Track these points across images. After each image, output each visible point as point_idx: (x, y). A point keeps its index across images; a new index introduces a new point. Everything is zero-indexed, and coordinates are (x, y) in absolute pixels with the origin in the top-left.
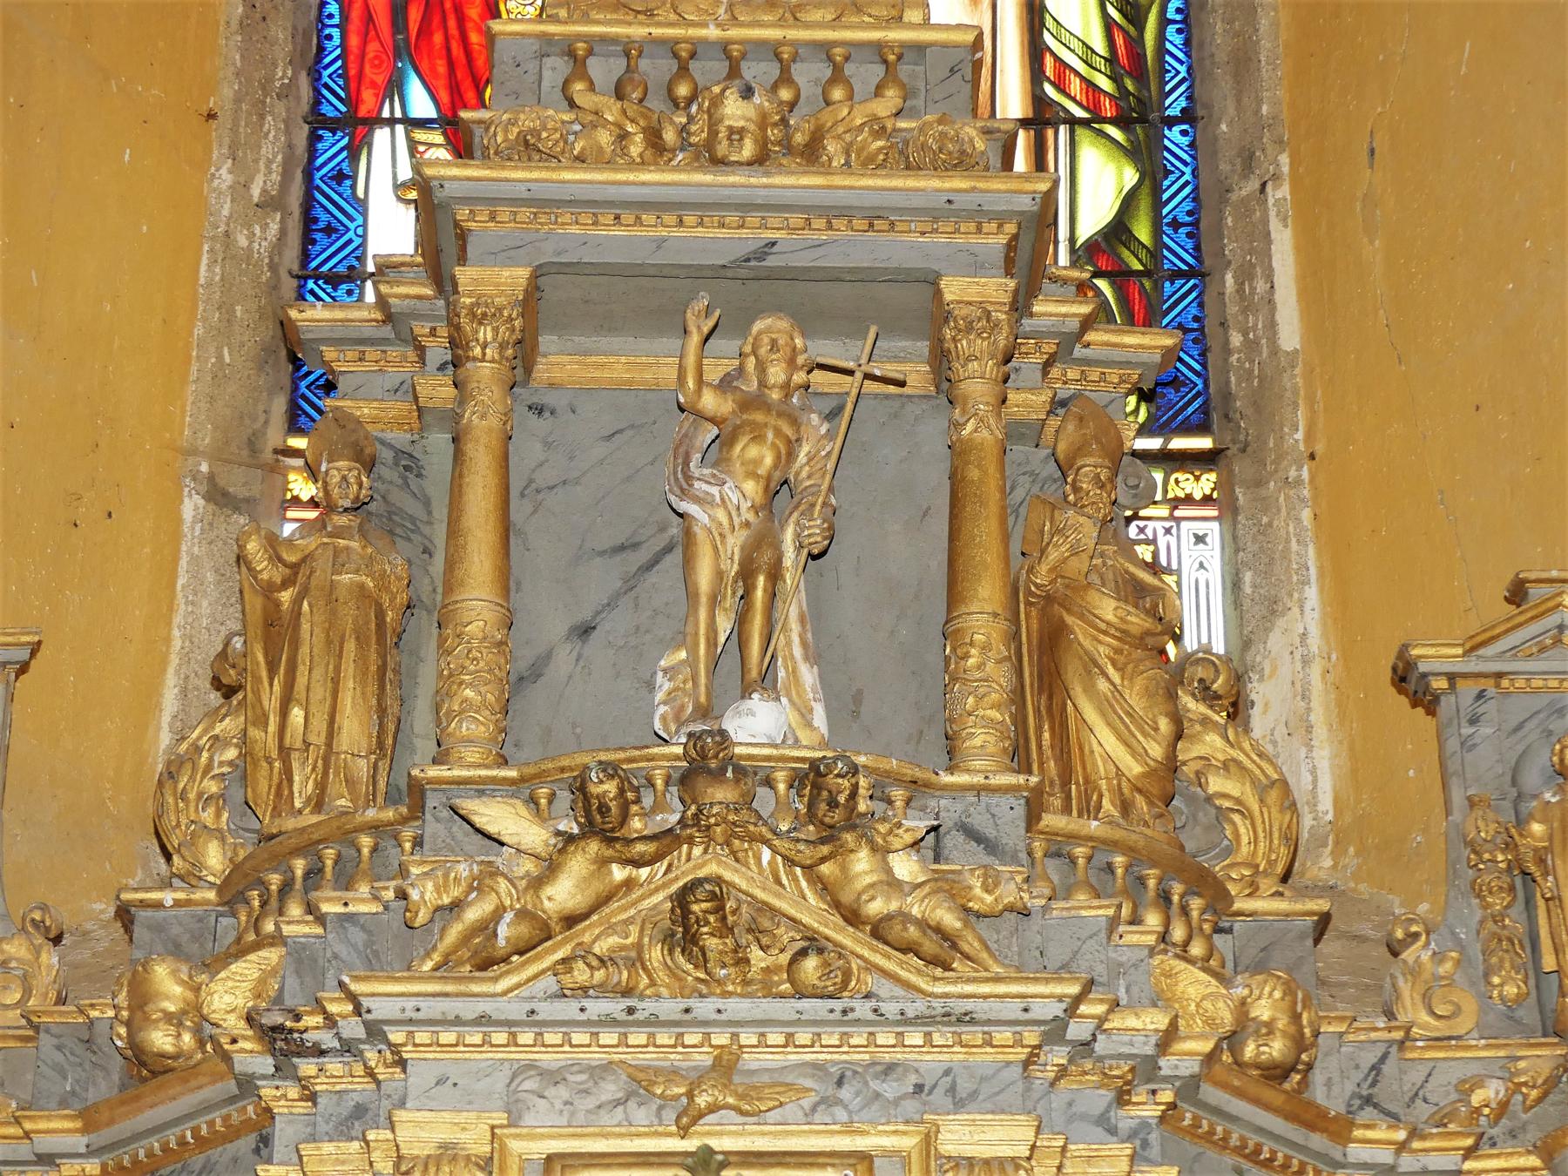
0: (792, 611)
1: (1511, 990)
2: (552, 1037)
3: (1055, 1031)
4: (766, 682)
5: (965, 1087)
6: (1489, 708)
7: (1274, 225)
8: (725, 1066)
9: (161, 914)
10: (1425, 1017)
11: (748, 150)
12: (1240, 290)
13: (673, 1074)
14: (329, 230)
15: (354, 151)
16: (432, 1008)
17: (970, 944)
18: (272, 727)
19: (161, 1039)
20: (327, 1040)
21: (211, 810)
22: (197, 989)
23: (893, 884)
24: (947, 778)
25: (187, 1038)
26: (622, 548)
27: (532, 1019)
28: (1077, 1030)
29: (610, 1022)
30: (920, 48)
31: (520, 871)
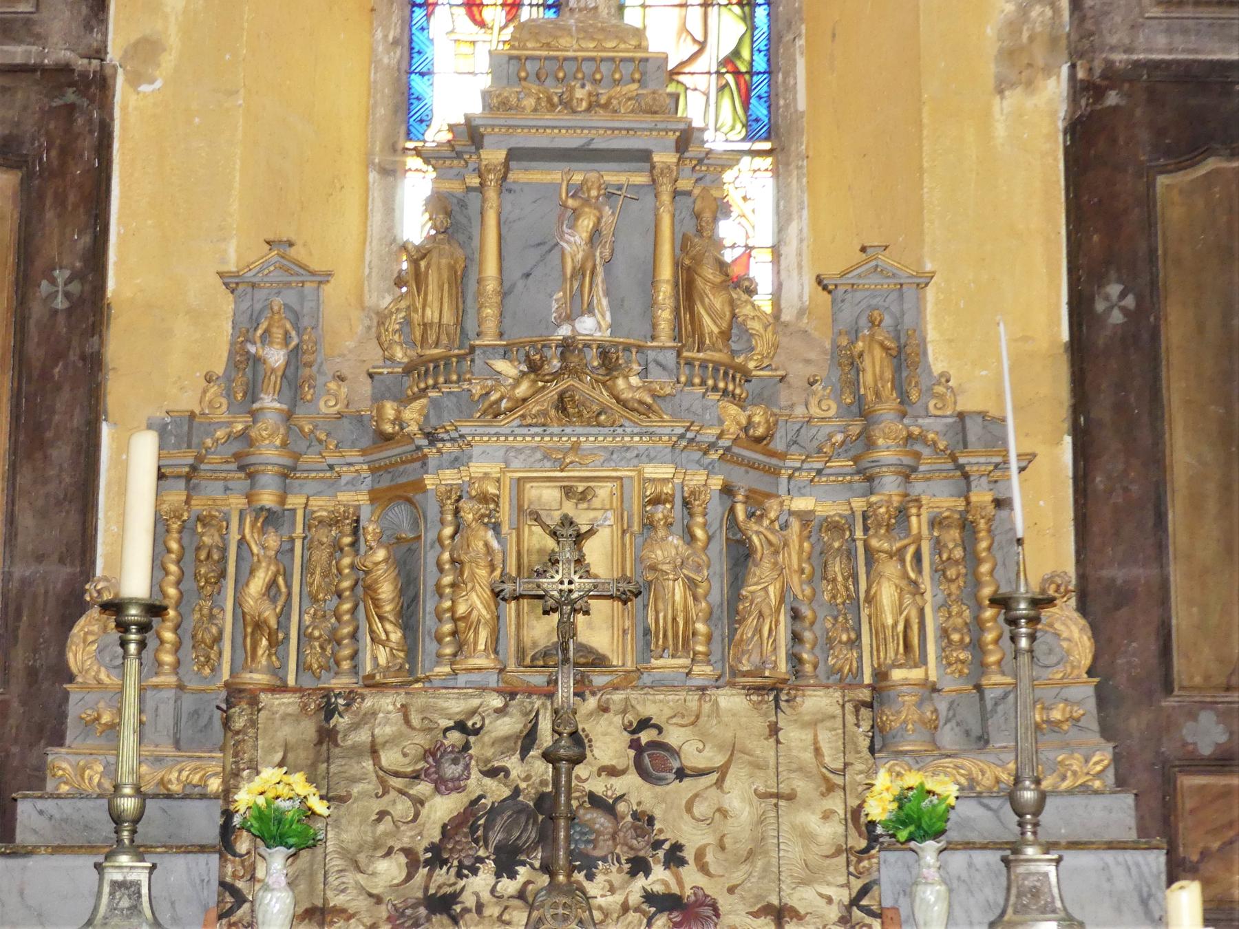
0: (599, 279)
1: (848, 401)
2: (519, 439)
3: (682, 436)
4: (590, 311)
5: (653, 454)
6: (849, 296)
7: (798, 57)
8: (575, 448)
9: (381, 377)
10: (818, 410)
11: (584, 105)
12: (784, 81)
13: (558, 450)
14: (419, 52)
15: (428, 16)
16: (480, 430)
17: (655, 407)
18: (420, 313)
19: (388, 428)
20: (446, 437)
21: (397, 335)
22: (400, 412)
23: (630, 386)
24: (649, 344)
25: (397, 428)
26: (539, 244)
27: (512, 433)
28: (690, 435)
29: (537, 434)
30: (647, 60)
31: (507, 383)
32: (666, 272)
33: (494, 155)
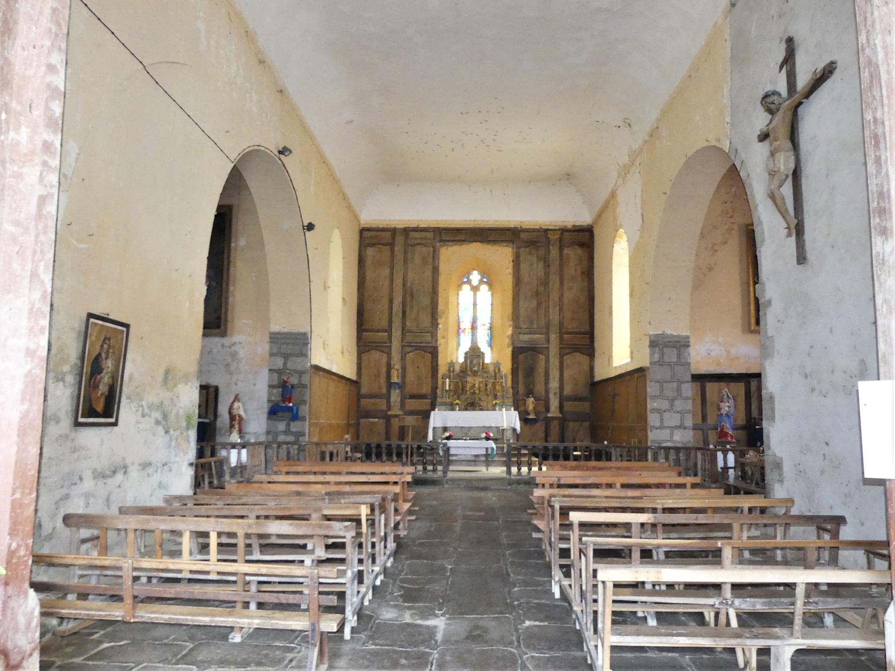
32: (481, 364)
33: (468, 356)
